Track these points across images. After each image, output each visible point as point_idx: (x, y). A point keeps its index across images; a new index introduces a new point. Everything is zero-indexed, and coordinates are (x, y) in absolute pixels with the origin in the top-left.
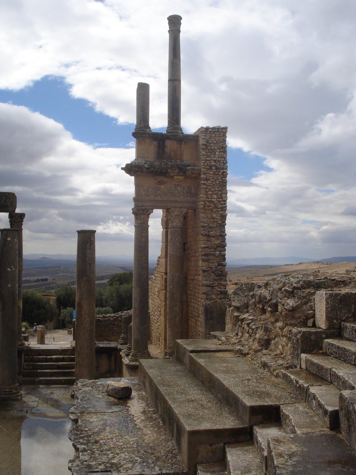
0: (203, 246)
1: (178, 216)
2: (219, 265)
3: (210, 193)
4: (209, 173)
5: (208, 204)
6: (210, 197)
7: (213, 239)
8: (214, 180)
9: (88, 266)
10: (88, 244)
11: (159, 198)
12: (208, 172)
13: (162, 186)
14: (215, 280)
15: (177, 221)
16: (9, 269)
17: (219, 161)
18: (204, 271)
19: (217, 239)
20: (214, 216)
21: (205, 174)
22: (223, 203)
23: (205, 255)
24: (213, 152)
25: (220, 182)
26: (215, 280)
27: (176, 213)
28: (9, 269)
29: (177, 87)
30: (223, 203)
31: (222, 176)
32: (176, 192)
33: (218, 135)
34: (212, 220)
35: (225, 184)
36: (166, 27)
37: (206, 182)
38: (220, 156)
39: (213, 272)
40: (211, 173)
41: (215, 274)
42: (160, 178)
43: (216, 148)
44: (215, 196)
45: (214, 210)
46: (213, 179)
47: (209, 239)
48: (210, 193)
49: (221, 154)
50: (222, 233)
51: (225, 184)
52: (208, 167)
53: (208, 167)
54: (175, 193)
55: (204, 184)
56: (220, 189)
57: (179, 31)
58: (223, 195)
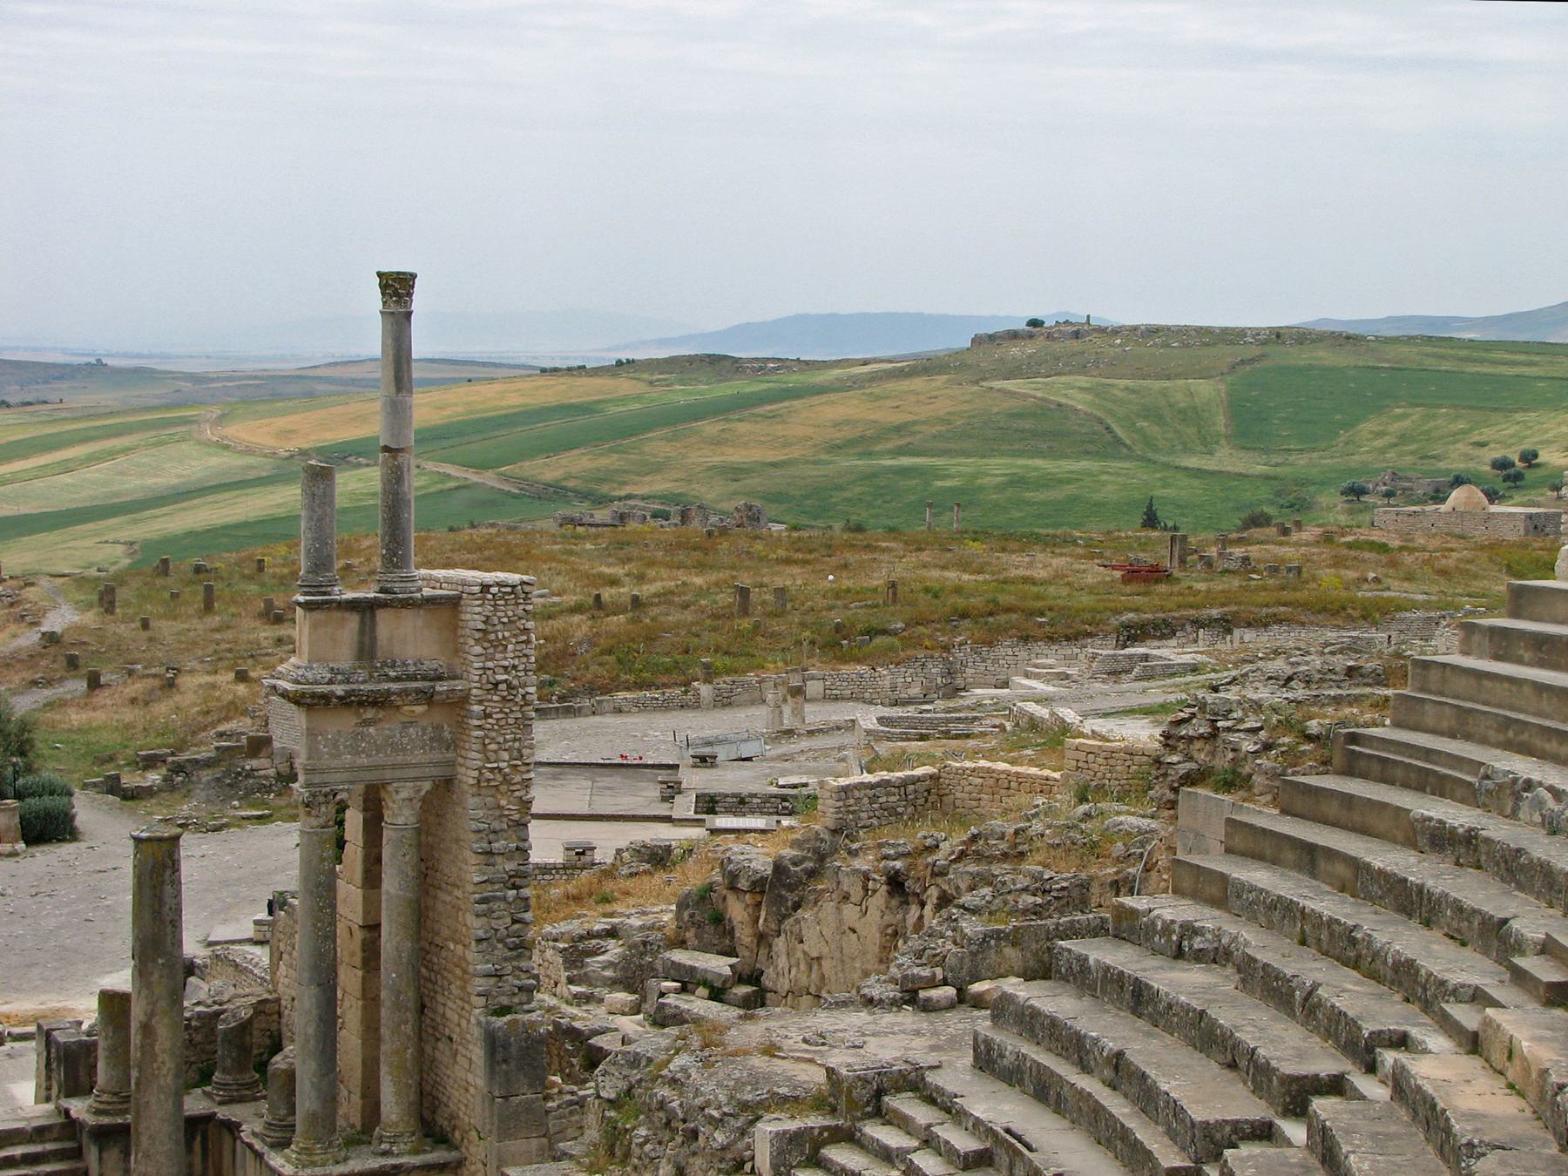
0: (477, 879)
1: (411, 800)
2: (514, 922)
3: (493, 747)
5: (488, 775)
6: (492, 756)
7: (499, 859)
9: (169, 928)
10: (168, 872)
11: (363, 760)
13: (372, 730)
14: (506, 959)
15: (407, 812)
17: (514, 667)
18: (479, 941)
19: (510, 859)
20: (503, 802)
21: (480, 702)
23: (484, 901)
26: (506, 959)
27: (404, 794)
34: (497, 813)
36: (374, 299)
39: (499, 941)
41: (506, 945)
42: (370, 713)
44: (506, 756)
45: (503, 788)
48: (493, 747)
50: (521, 845)
55: (479, 727)
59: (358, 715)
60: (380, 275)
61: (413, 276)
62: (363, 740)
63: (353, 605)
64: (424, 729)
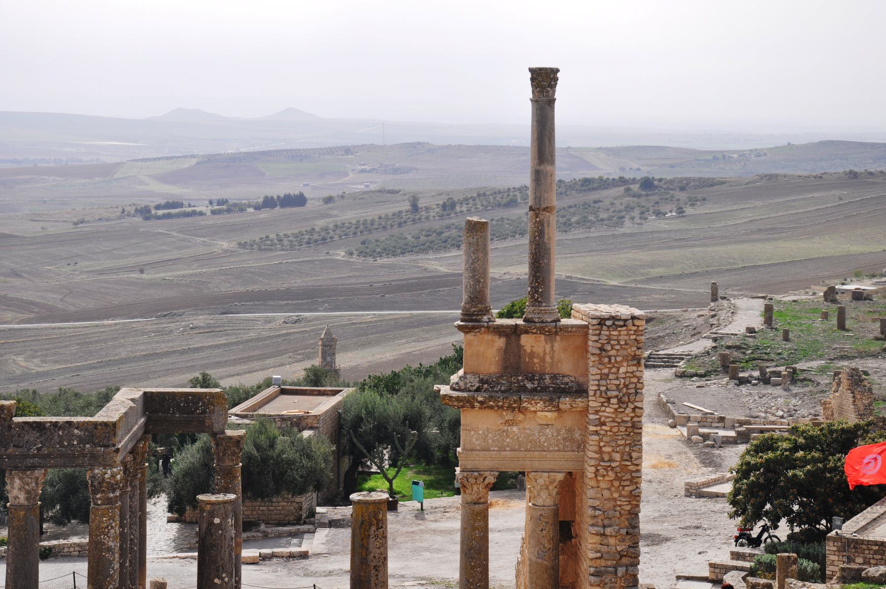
4: (604, 411)
6: (606, 457)
8: (616, 424)
9: (373, 571)
10: (374, 528)
12: (603, 408)
13: (515, 429)
15: (544, 494)
16: (216, 581)
17: (626, 386)
21: (597, 412)
22: (632, 468)
24: (614, 366)
25: (627, 427)
28: (216, 581)
29: (546, 225)
30: (632, 468)
31: (633, 415)
32: (543, 439)
33: (626, 332)
35: (638, 431)
36: (526, 90)
37: (598, 428)
38: (628, 375)
40: (608, 410)
43: (619, 359)
46: (614, 421)
47: (605, 542)
49: (630, 369)
50: (631, 531)
51: (638, 431)
52: (603, 400)
53: (603, 400)
54: (540, 442)
55: (596, 433)
56: (628, 442)
57: (551, 102)
58: (634, 455)
59: (501, 416)
60: (531, 70)
61: (558, 70)
62: (508, 436)
63: (500, 331)
64: (558, 431)
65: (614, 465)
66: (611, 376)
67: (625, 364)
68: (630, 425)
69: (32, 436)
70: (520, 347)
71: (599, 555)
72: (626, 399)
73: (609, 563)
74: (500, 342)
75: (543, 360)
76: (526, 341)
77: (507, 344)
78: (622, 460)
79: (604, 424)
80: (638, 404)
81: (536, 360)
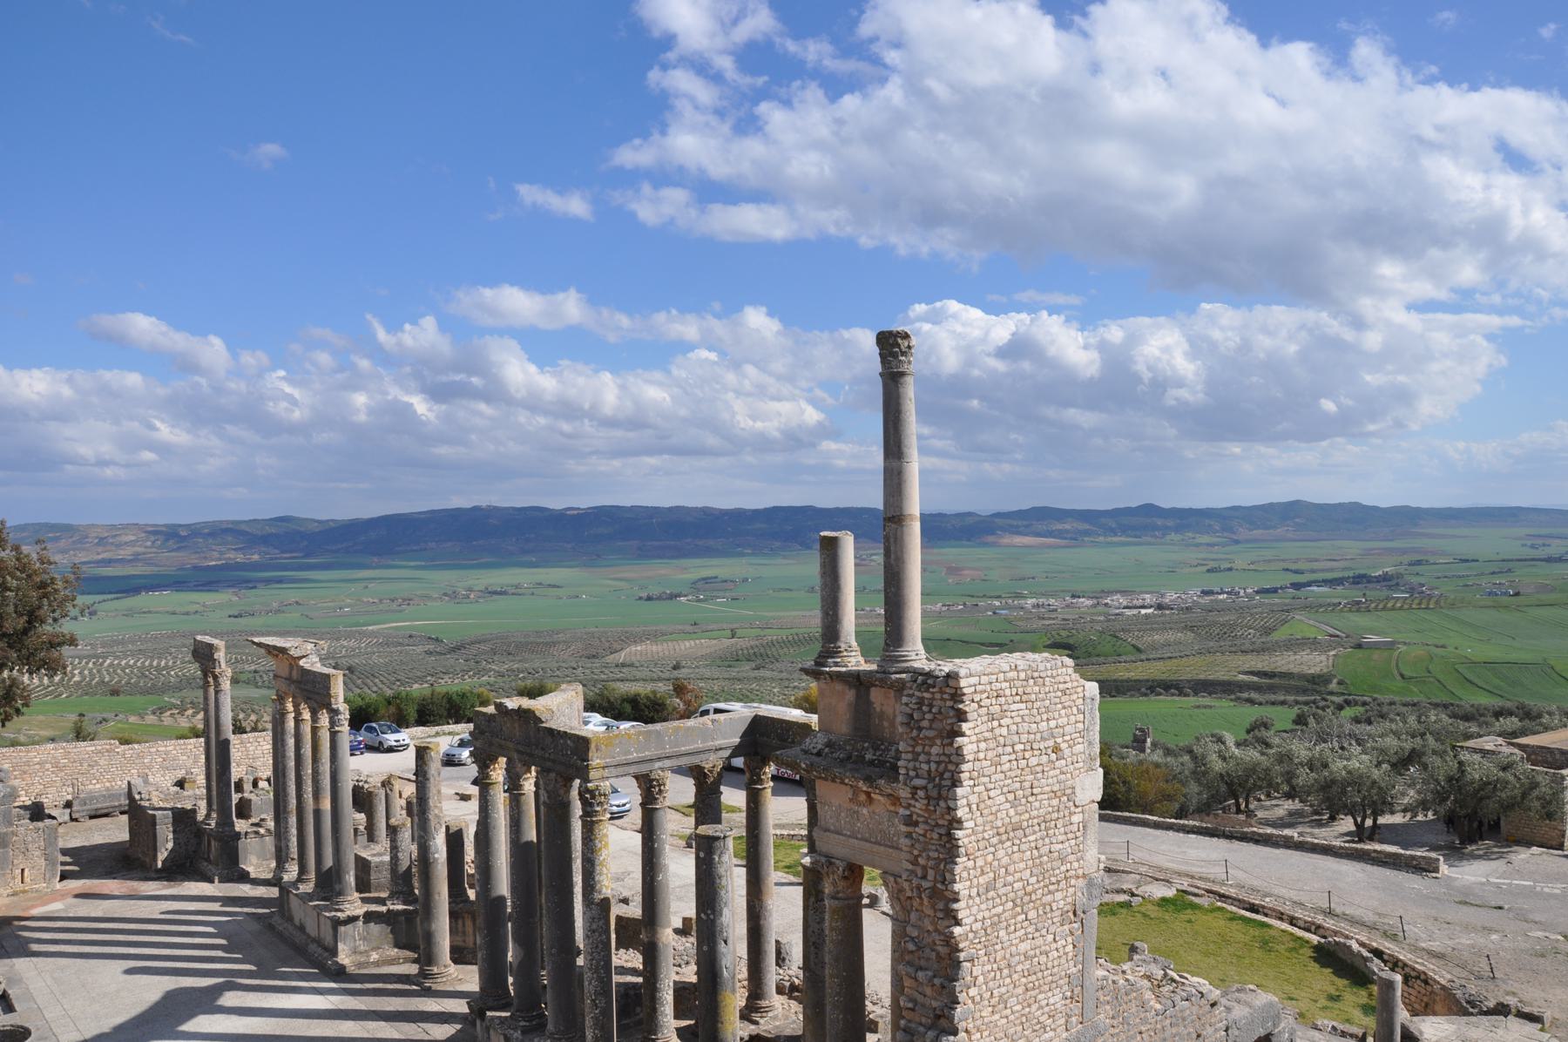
13: (865, 811)
46: (926, 822)
58: (948, 876)
65: (926, 884)
66: (922, 758)
67: (938, 742)
68: (943, 831)
69: (549, 740)
70: (869, 703)
71: (910, 1005)
72: (934, 793)
73: (923, 1020)
74: (850, 695)
75: (892, 724)
76: (876, 695)
77: (858, 696)
78: (935, 881)
79: (916, 824)
80: (951, 804)
81: (886, 724)
